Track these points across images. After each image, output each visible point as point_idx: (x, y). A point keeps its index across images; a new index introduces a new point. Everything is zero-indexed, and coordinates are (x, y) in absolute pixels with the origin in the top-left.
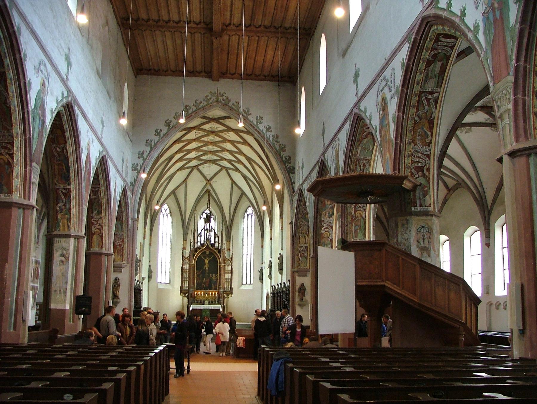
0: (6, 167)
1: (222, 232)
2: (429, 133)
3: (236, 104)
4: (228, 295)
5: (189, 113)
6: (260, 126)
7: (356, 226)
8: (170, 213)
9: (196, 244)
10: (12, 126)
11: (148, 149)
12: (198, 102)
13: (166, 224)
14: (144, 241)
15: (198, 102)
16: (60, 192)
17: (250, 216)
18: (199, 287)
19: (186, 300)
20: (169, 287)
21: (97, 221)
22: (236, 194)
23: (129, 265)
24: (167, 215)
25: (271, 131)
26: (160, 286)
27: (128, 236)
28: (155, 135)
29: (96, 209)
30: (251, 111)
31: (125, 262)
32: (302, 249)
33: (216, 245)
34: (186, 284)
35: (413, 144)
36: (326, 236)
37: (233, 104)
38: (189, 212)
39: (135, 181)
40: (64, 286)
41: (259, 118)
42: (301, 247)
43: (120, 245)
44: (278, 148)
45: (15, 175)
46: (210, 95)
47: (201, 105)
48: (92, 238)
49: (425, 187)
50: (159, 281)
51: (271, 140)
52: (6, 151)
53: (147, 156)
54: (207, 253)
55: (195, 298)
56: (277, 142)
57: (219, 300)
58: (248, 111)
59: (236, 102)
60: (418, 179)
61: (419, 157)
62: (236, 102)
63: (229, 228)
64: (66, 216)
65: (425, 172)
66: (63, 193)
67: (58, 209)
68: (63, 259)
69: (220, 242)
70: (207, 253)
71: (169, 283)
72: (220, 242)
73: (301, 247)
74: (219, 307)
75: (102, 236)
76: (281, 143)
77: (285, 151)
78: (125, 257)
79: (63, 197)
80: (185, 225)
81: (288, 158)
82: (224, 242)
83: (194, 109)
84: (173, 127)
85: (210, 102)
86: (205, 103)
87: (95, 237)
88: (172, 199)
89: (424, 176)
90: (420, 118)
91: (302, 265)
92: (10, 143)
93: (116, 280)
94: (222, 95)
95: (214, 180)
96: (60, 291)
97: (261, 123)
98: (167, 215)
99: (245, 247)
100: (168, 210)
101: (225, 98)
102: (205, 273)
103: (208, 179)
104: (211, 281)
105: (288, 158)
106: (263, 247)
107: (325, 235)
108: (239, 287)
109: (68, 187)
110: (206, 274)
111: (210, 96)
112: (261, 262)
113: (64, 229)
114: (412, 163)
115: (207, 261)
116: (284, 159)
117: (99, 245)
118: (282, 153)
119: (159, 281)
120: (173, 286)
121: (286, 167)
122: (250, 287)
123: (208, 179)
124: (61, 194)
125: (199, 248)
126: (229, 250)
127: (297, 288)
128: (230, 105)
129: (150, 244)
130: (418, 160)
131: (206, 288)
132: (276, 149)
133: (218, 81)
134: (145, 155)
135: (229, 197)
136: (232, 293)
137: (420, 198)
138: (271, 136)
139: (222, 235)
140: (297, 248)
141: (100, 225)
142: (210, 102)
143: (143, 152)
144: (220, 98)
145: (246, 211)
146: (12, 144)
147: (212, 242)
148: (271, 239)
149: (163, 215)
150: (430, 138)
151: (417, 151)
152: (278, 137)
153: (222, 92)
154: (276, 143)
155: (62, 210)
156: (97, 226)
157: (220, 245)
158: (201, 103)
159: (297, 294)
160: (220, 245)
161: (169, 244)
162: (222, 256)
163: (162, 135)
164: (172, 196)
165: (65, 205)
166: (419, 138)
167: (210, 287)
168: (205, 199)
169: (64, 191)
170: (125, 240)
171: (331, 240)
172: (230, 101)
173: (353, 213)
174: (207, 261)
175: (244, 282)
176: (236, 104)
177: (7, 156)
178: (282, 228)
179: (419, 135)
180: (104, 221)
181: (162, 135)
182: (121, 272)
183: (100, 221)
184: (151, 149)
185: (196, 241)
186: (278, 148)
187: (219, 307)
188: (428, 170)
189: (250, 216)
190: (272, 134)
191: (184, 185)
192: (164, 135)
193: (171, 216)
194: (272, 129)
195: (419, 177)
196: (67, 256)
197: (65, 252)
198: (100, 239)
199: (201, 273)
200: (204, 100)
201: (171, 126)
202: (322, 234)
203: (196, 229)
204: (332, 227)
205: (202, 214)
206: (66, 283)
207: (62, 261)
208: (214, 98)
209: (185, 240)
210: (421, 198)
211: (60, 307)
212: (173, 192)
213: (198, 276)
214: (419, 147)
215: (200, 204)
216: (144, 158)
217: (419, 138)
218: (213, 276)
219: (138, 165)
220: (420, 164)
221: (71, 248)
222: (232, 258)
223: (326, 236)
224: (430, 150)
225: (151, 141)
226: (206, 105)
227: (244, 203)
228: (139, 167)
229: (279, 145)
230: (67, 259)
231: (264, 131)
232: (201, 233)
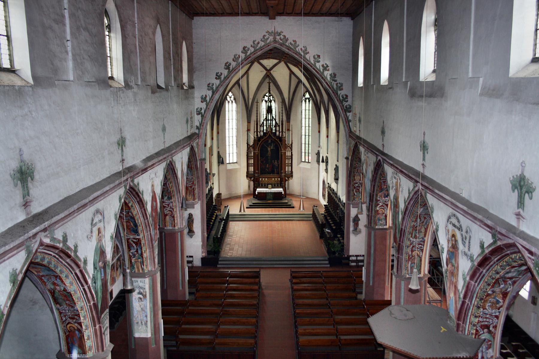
0: (77, 332)
1: (282, 121)
2: (501, 301)
3: (293, 43)
4: (288, 178)
5: (248, 54)
6: (318, 65)
7: (411, 263)
8: (235, 99)
9: (259, 133)
10: (75, 304)
11: (210, 93)
12: (256, 43)
13: (232, 111)
15: (256, 43)
16: (130, 241)
17: (307, 101)
19: (252, 183)
20: (236, 166)
21: (168, 205)
22: (294, 81)
23: (200, 202)
24: (232, 102)
25: (328, 70)
26: (229, 167)
27: (198, 177)
28: (216, 78)
29: (166, 196)
30: (308, 50)
31: (197, 200)
32: (357, 185)
33: (277, 133)
34: (252, 169)
35: (482, 309)
36: (381, 212)
37: (291, 43)
38: (251, 97)
39: (200, 125)
40: (145, 318)
41: (316, 57)
42: (357, 183)
43: (191, 187)
44: (335, 86)
45: (86, 338)
46: (267, 34)
47: (259, 45)
48: (165, 218)
49: (490, 341)
50: (228, 162)
51: (329, 79)
52: (74, 321)
53: (210, 100)
54: (270, 142)
55: (261, 183)
56: (335, 81)
57: (281, 184)
58: (306, 50)
59: (294, 41)
60: (482, 336)
61: (486, 318)
62: (294, 41)
63: (288, 109)
64: (139, 260)
65: (491, 329)
66: (134, 242)
67: (131, 254)
68: (141, 296)
69: (281, 131)
70: (270, 142)
71: (236, 163)
72: (281, 131)
73: (357, 183)
74: (281, 190)
75: (174, 217)
76: (338, 82)
77: (342, 89)
78: (196, 196)
79: (134, 245)
80: (249, 109)
81: (345, 96)
82: (284, 130)
83: (252, 50)
84: (233, 69)
85: (268, 41)
86: (263, 44)
87: (168, 217)
89: (490, 332)
90: (493, 292)
91: (356, 199)
92: (76, 315)
93: (191, 216)
94: (280, 34)
95: (274, 69)
96: (142, 323)
97: (319, 62)
98: (232, 102)
99: (303, 128)
100: (233, 97)
101: (282, 37)
103: (268, 68)
105: (345, 96)
106: (319, 132)
107: (380, 212)
108: (298, 164)
109: (137, 237)
110: (269, 161)
111: (267, 36)
112: (318, 145)
113: (139, 270)
114: (478, 323)
116: (341, 98)
117: (172, 224)
118: (339, 92)
119: (228, 162)
120: (240, 165)
121: (343, 106)
122: (307, 166)
123: (268, 68)
124: (132, 243)
125: (261, 137)
126: (288, 130)
127: (351, 219)
128: (287, 44)
129: (218, 133)
130: (485, 320)
132: (333, 88)
133: (274, 19)
134: (208, 99)
135: (288, 83)
136: (292, 176)
137: (482, 351)
138: (329, 75)
139: (282, 124)
140: (352, 183)
141: (171, 208)
142: (268, 41)
143: (206, 96)
144: (278, 37)
145: (304, 96)
146: (78, 315)
147: (274, 131)
148: (327, 137)
149: (229, 102)
150: (501, 304)
151: (485, 314)
152: (335, 75)
153: (279, 32)
154: (333, 82)
155: (134, 256)
156: (169, 209)
157: (281, 133)
158: (258, 43)
159: (352, 224)
160: (281, 133)
161: (235, 127)
162: (283, 144)
163: (222, 79)
164: (237, 85)
165: (137, 251)
166: (490, 304)
167: (273, 172)
168: (265, 85)
169: (134, 240)
170: (196, 182)
171: (386, 216)
172: (287, 40)
173: (410, 253)
174: (269, 149)
175: (303, 160)
176: (293, 43)
177: (76, 324)
178: (338, 142)
179: (490, 302)
180: (174, 204)
181: (222, 79)
182: (194, 208)
183: (171, 205)
184: (213, 93)
185: (259, 130)
186: (335, 86)
187: (281, 190)
188: (495, 327)
189: (307, 101)
190: (330, 72)
191: (246, 76)
192: (225, 78)
193: (236, 102)
194: (330, 68)
195: (484, 333)
196: (144, 294)
197: (142, 291)
198: (172, 219)
200: (262, 40)
201: (231, 68)
202: (378, 211)
203: (259, 120)
204: (387, 205)
205: (264, 97)
206: (146, 316)
207: (141, 298)
208: (271, 38)
209: (249, 122)
210: (484, 351)
211: (143, 335)
212: (237, 82)
213: (262, 162)
214: (489, 310)
215: (261, 89)
216: (206, 102)
217: (490, 304)
219: (201, 109)
220: (486, 323)
221: (147, 287)
222: (292, 145)
223: (381, 212)
224: (500, 312)
225: (213, 84)
226: (264, 46)
227: (302, 89)
228: (203, 111)
229: (337, 84)
230: (145, 296)
231: (322, 70)
232: (263, 123)
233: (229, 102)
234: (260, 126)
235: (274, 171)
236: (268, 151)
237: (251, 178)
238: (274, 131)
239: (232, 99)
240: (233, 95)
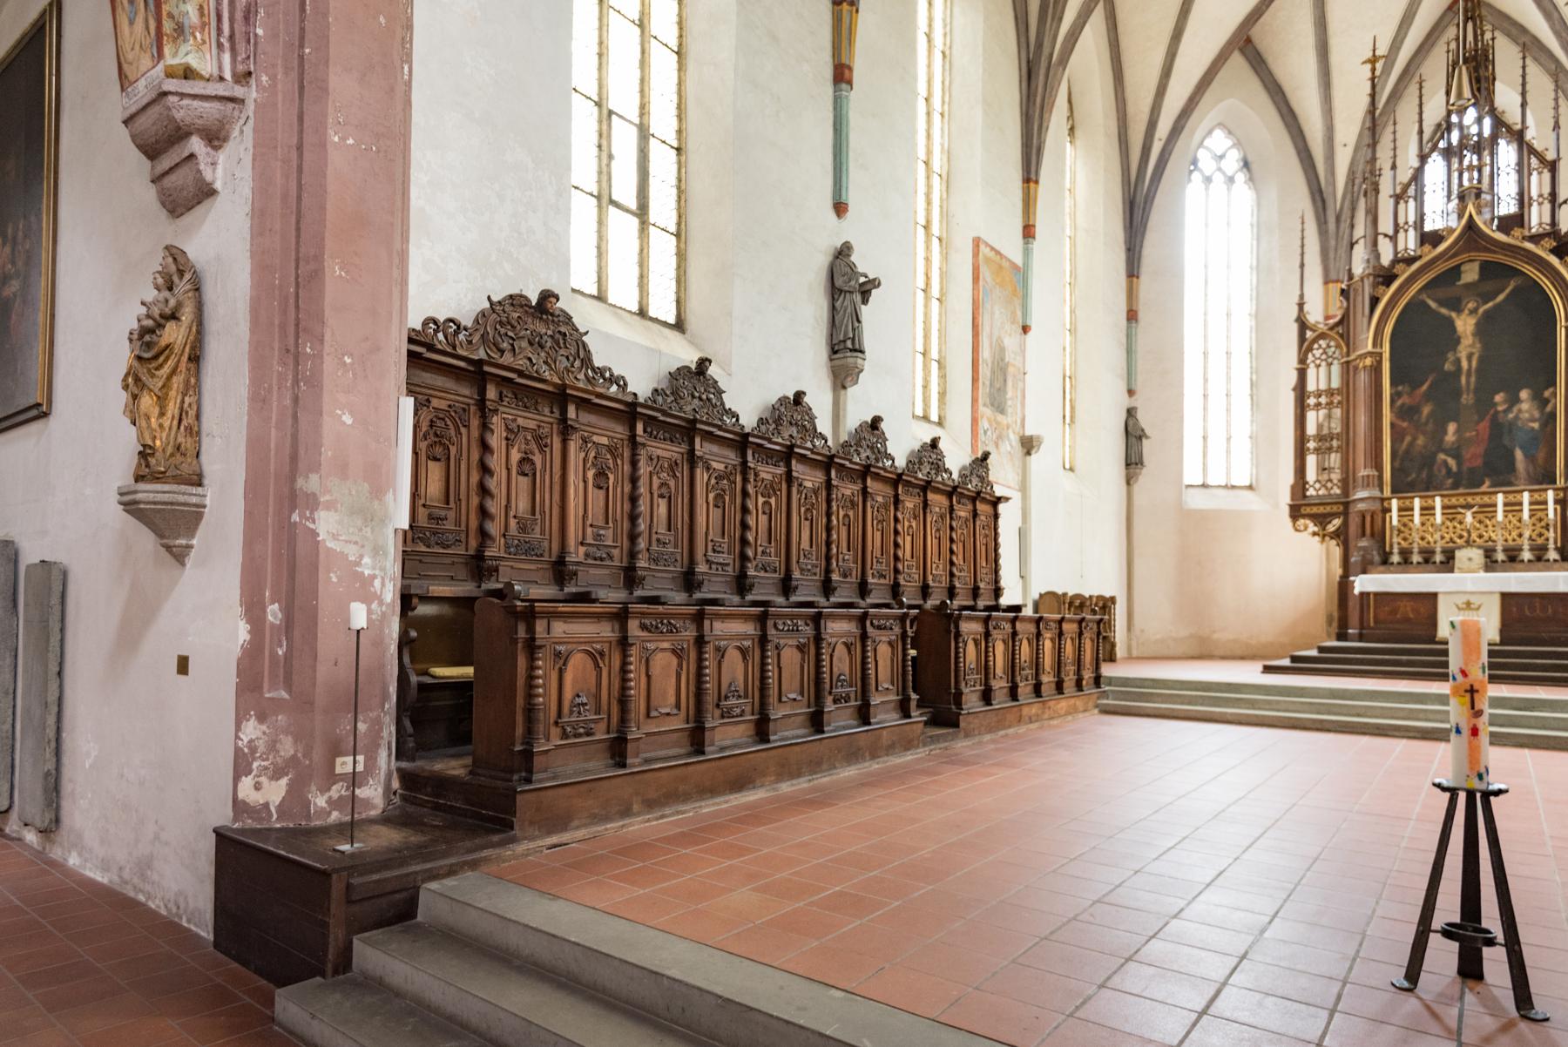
8: (1246, 165)
14: (1027, 253)
18: (1414, 476)
33: (1537, 217)
54: (1470, 274)
88: (1239, 95)
98: (1231, 180)
102: (1457, 393)
104: (1500, 431)
110: (1467, 399)
115: (1465, 324)
131: (1466, 480)
149: (1208, 180)
164: (1237, 60)
167: (1498, 470)
174: (1465, 324)
193: (1251, 179)
199: (1428, 397)
212: (1245, 45)
213: (1405, 413)
218: (1514, 400)
233: (1208, 180)
234: (1398, 198)
235: (1511, 466)
236: (1458, 341)
237: (1321, 520)
238: (1507, 207)
239: (1232, 162)
240: (1238, 144)
